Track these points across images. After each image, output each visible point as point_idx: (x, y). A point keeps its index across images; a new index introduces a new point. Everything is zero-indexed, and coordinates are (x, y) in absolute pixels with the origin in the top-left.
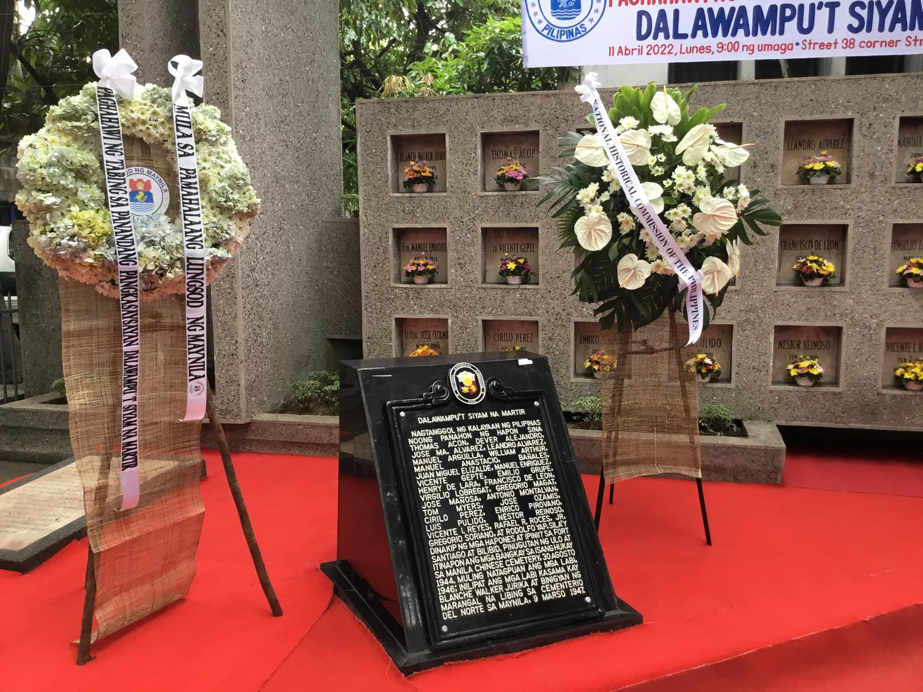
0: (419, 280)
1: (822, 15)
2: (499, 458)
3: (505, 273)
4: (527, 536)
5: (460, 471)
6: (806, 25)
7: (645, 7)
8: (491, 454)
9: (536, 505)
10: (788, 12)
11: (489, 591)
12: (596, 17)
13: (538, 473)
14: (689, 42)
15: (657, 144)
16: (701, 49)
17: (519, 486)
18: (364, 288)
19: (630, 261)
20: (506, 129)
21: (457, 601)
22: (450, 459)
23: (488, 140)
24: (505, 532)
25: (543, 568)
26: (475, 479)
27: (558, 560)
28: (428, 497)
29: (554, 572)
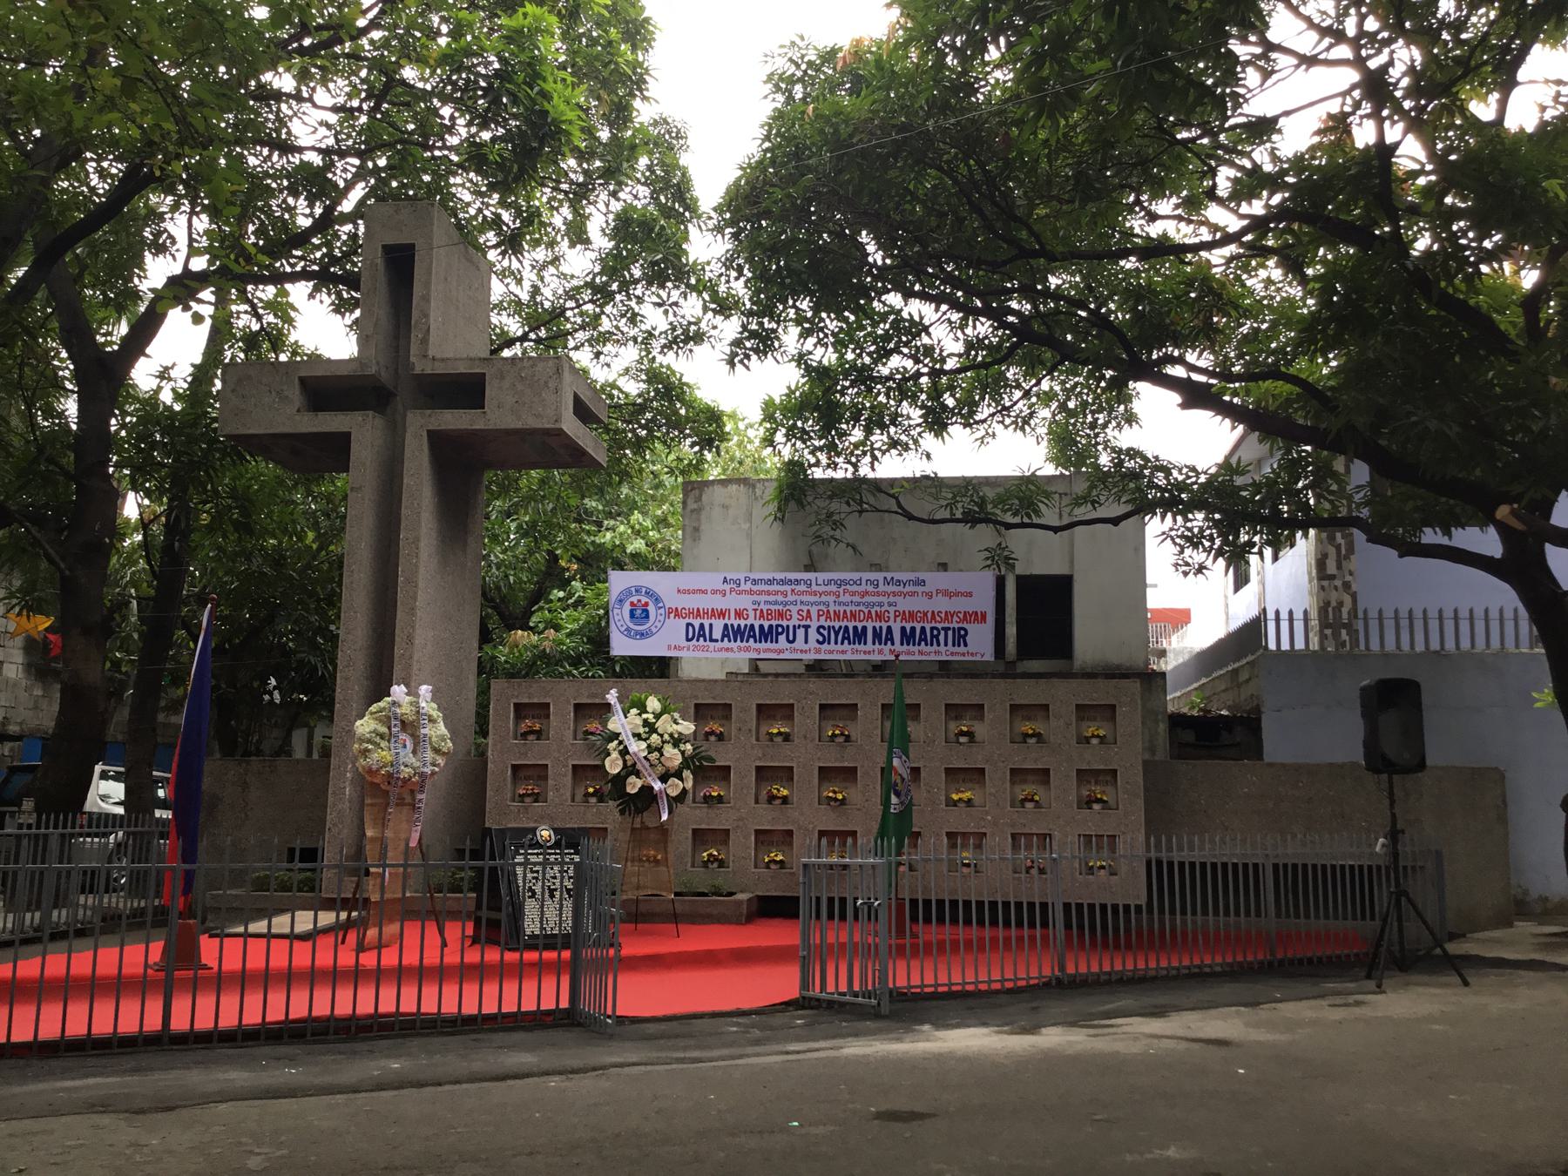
0: (528, 800)
1: (800, 633)
3: (587, 795)
6: (791, 638)
7: (691, 621)
10: (780, 630)
12: (659, 625)
14: (719, 645)
15: (646, 723)
16: (727, 650)
18: (488, 806)
19: (632, 779)
20: (589, 701)
23: (578, 707)
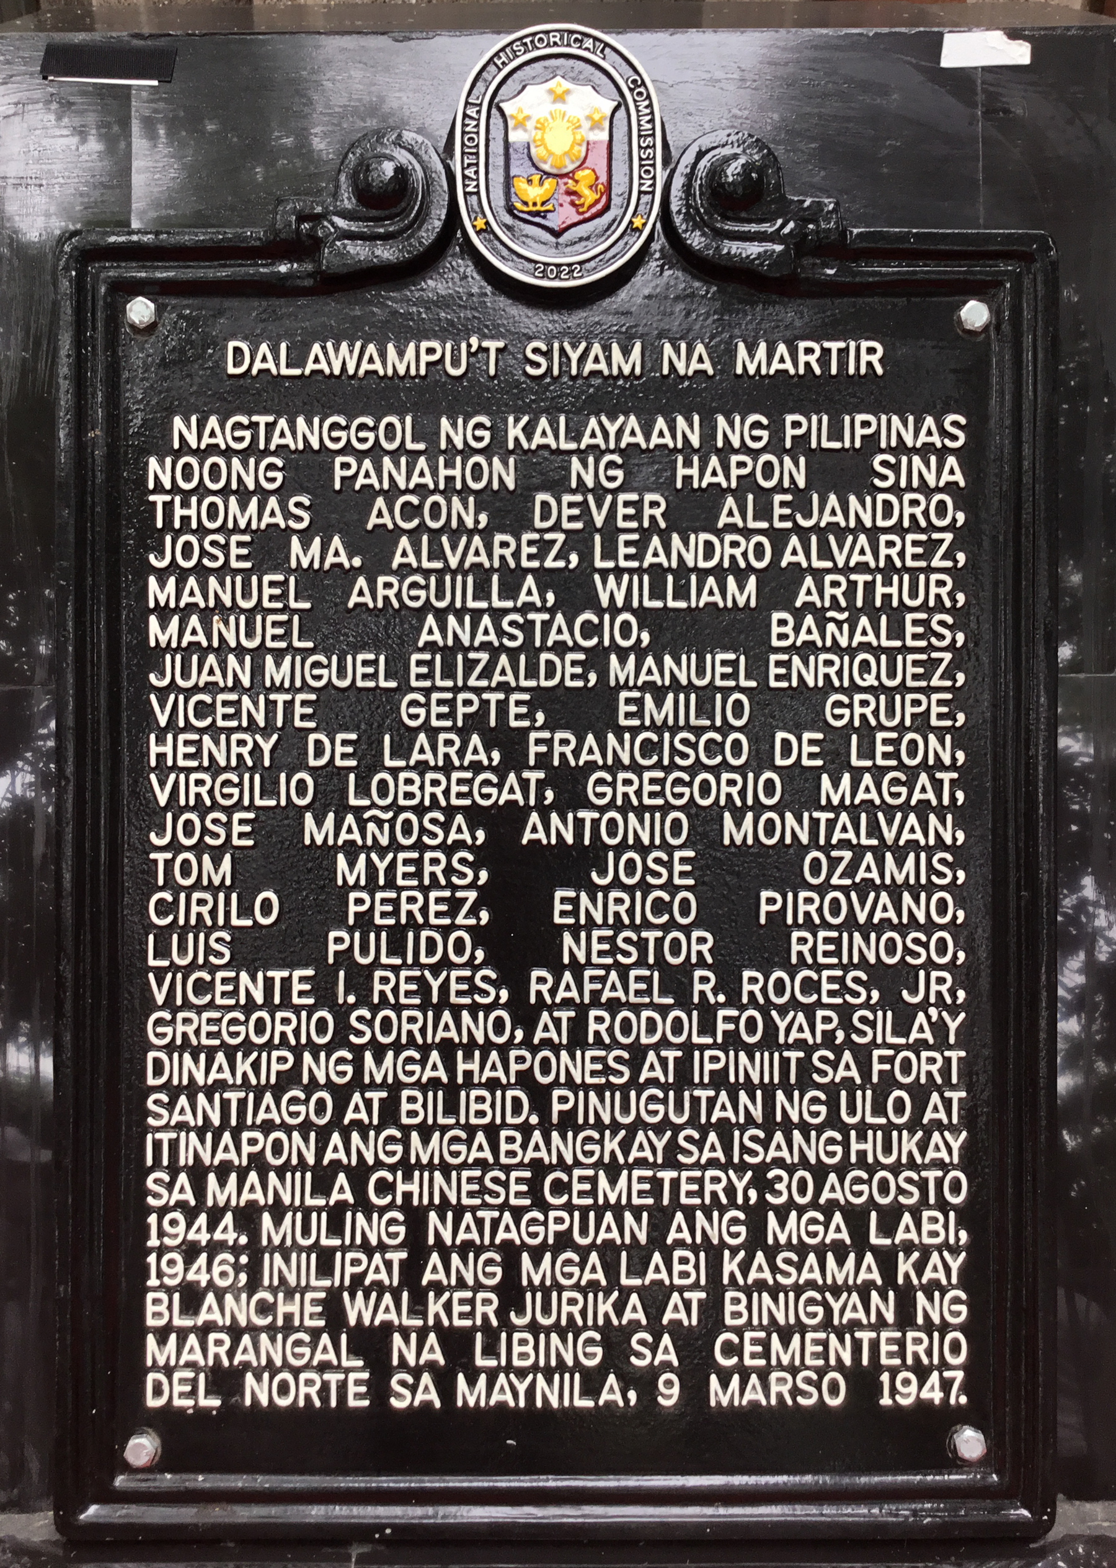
2: (642, 614)
4: (705, 1065)
5: (398, 669)
8: (608, 591)
9: (806, 904)
11: (418, 1306)
13: (867, 732)
17: (726, 788)
21: (235, 1332)
22: (359, 594)
24: (578, 1026)
25: (757, 1239)
26: (476, 722)
27: (856, 1218)
28: (196, 787)
29: (811, 1272)
